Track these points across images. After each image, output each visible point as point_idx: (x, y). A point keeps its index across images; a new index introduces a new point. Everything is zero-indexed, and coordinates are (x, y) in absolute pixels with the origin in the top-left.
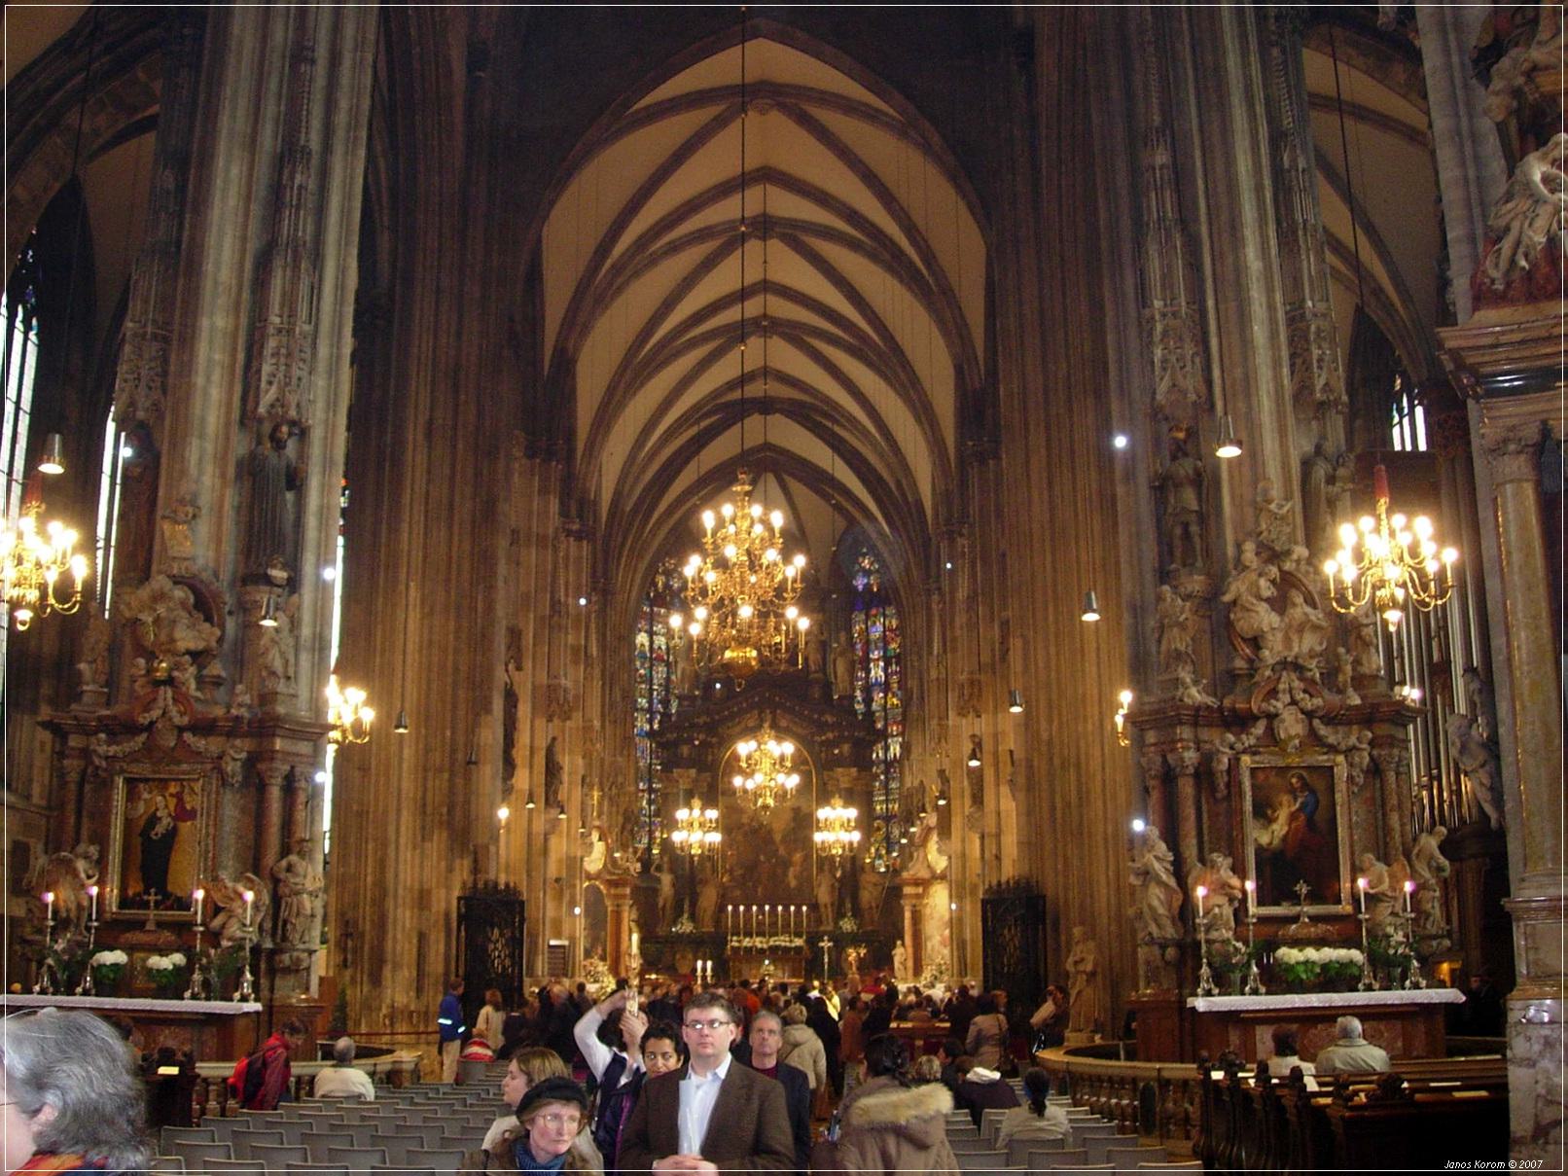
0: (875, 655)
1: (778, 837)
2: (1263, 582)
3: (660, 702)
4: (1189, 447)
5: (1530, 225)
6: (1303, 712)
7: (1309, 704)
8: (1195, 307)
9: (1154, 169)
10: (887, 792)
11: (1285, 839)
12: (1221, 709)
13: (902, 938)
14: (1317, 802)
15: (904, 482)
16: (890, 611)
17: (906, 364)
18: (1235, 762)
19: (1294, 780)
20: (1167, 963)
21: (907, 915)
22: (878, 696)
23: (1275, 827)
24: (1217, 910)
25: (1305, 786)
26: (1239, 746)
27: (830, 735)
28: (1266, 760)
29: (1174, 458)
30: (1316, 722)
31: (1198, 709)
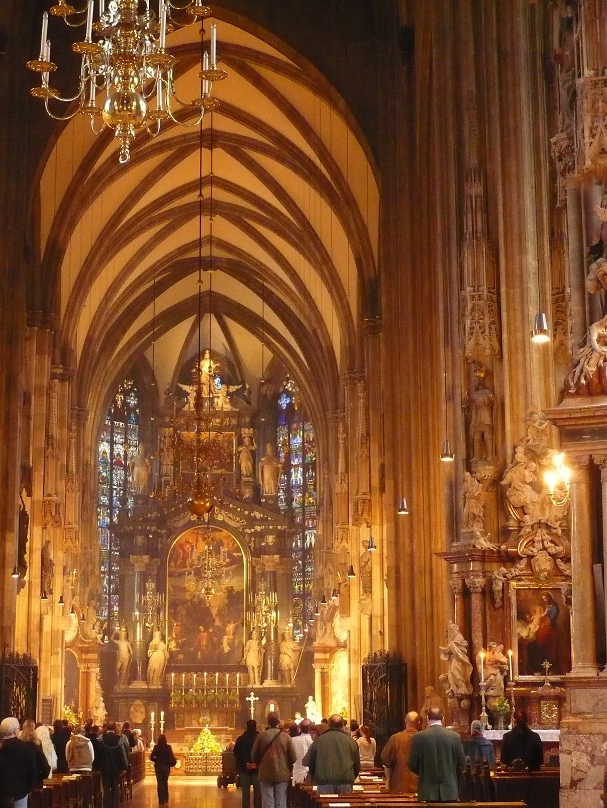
0: (295, 462)
1: (214, 611)
2: (527, 472)
3: (119, 500)
4: (487, 383)
5: (588, 363)
6: (550, 555)
7: (553, 550)
8: (494, 291)
9: (471, 197)
10: (304, 574)
11: (537, 633)
12: (499, 552)
13: (314, 696)
14: (558, 610)
15: (319, 332)
16: (308, 426)
17: (320, 247)
18: (506, 586)
19: (544, 597)
20: (462, 709)
21: (318, 676)
22: (298, 496)
23: (531, 626)
24: (492, 677)
25: (550, 600)
26: (509, 576)
27: (258, 528)
28: (526, 584)
29: (477, 389)
30: (559, 561)
31: (484, 552)
